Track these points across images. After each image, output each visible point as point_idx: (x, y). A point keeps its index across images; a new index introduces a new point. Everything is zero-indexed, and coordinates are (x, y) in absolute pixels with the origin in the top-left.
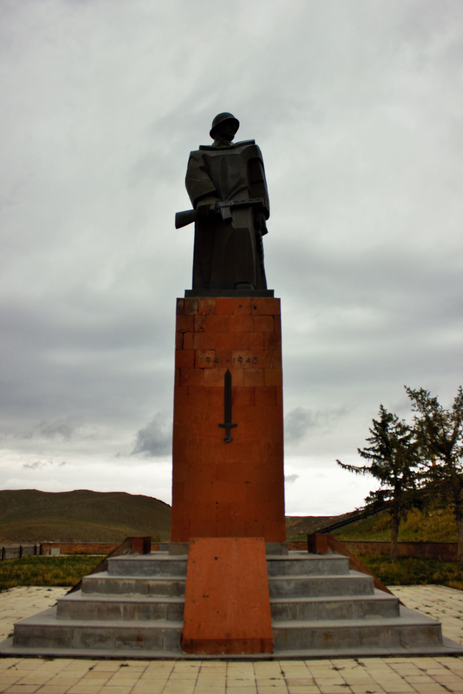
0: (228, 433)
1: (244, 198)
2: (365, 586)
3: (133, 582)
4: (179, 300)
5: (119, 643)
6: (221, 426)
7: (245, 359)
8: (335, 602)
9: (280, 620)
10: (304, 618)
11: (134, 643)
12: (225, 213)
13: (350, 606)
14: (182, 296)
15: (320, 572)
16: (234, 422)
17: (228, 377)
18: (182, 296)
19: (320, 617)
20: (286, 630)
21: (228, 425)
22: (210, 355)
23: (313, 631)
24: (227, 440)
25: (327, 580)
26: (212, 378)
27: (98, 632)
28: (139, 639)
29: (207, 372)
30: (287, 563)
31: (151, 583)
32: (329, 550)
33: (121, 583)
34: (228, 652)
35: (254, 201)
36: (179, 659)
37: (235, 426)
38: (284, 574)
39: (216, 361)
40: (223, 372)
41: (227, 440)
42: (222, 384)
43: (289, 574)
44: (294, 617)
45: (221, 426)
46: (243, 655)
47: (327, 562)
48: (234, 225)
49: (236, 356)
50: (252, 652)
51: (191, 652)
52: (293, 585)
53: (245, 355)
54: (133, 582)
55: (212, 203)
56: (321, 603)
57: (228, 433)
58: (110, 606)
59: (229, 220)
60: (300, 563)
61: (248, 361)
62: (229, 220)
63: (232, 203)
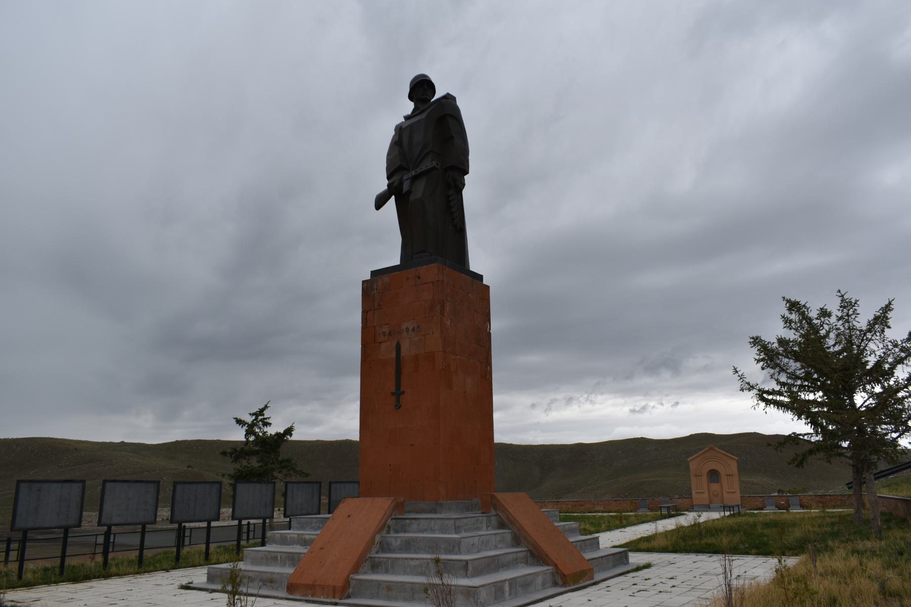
0: (398, 400)
1: (427, 164)
2: (454, 546)
3: (296, 536)
4: (364, 282)
5: (261, 584)
6: (393, 394)
7: (411, 329)
8: (417, 559)
9: (377, 573)
10: (394, 573)
11: (269, 584)
12: (406, 187)
13: (428, 564)
14: (368, 277)
15: (432, 530)
16: (402, 390)
17: (398, 348)
18: (368, 277)
19: (405, 573)
20: (361, 580)
21: (398, 393)
22: (386, 329)
23: (379, 583)
24: (398, 406)
25: (424, 538)
26: (386, 351)
27: (250, 574)
28: (271, 581)
29: (383, 345)
30: (408, 521)
31: (307, 537)
32: (492, 509)
33: (289, 536)
34: (313, 596)
35: (430, 167)
36: (282, 599)
37: (403, 393)
38: (405, 532)
39: (390, 334)
40: (394, 345)
41: (398, 406)
42: (394, 355)
43: (409, 532)
44: (387, 572)
45: (393, 394)
46: (322, 599)
47: (438, 521)
48: (412, 198)
49: (404, 327)
50: (328, 597)
51: (291, 594)
52: (399, 542)
53: (410, 325)
54: (296, 536)
55: (396, 178)
56: (406, 559)
57: (398, 400)
58: (273, 554)
59: (409, 192)
60: (417, 522)
61: (413, 330)
62: (409, 192)
63: (413, 173)
